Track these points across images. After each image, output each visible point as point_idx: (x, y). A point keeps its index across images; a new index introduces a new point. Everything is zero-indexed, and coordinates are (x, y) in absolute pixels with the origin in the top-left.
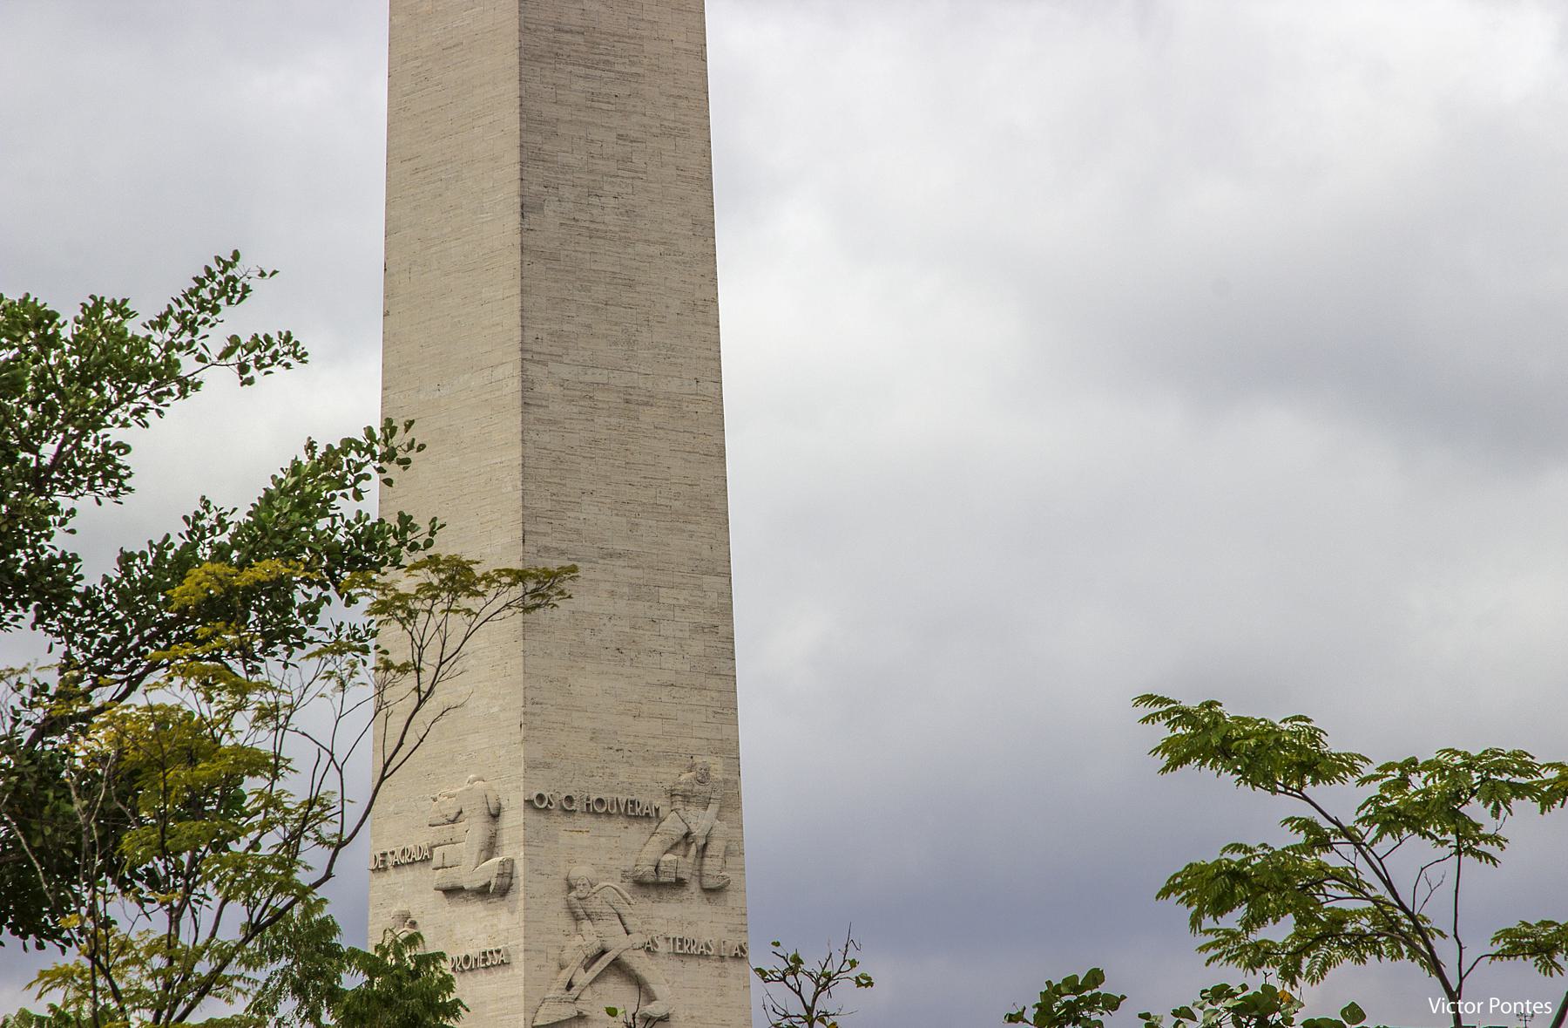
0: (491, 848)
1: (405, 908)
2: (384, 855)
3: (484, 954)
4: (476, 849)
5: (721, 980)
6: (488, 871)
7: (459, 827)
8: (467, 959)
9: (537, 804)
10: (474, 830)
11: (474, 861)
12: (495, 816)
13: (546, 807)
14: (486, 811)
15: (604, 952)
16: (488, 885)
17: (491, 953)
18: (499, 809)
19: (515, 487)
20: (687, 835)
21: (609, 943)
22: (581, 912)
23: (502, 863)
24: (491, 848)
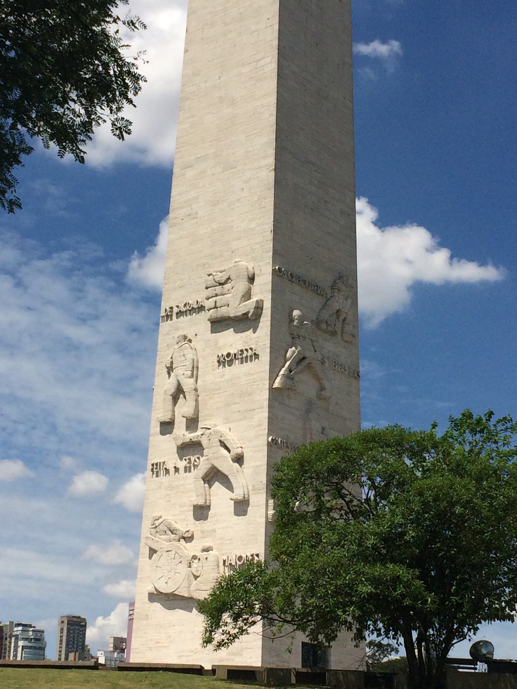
0: (247, 295)
1: (184, 333)
2: (171, 308)
3: (242, 351)
4: (240, 295)
5: (349, 388)
6: (249, 306)
7: (227, 286)
8: (229, 355)
9: (277, 274)
10: (241, 286)
11: (238, 303)
12: (251, 279)
13: (281, 276)
14: (247, 276)
15: (304, 358)
16: (246, 314)
17: (247, 350)
18: (254, 275)
19: (271, 115)
20: (338, 311)
21: (308, 354)
22: (295, 333)
23: (257, 302)
24: (247, 295)
